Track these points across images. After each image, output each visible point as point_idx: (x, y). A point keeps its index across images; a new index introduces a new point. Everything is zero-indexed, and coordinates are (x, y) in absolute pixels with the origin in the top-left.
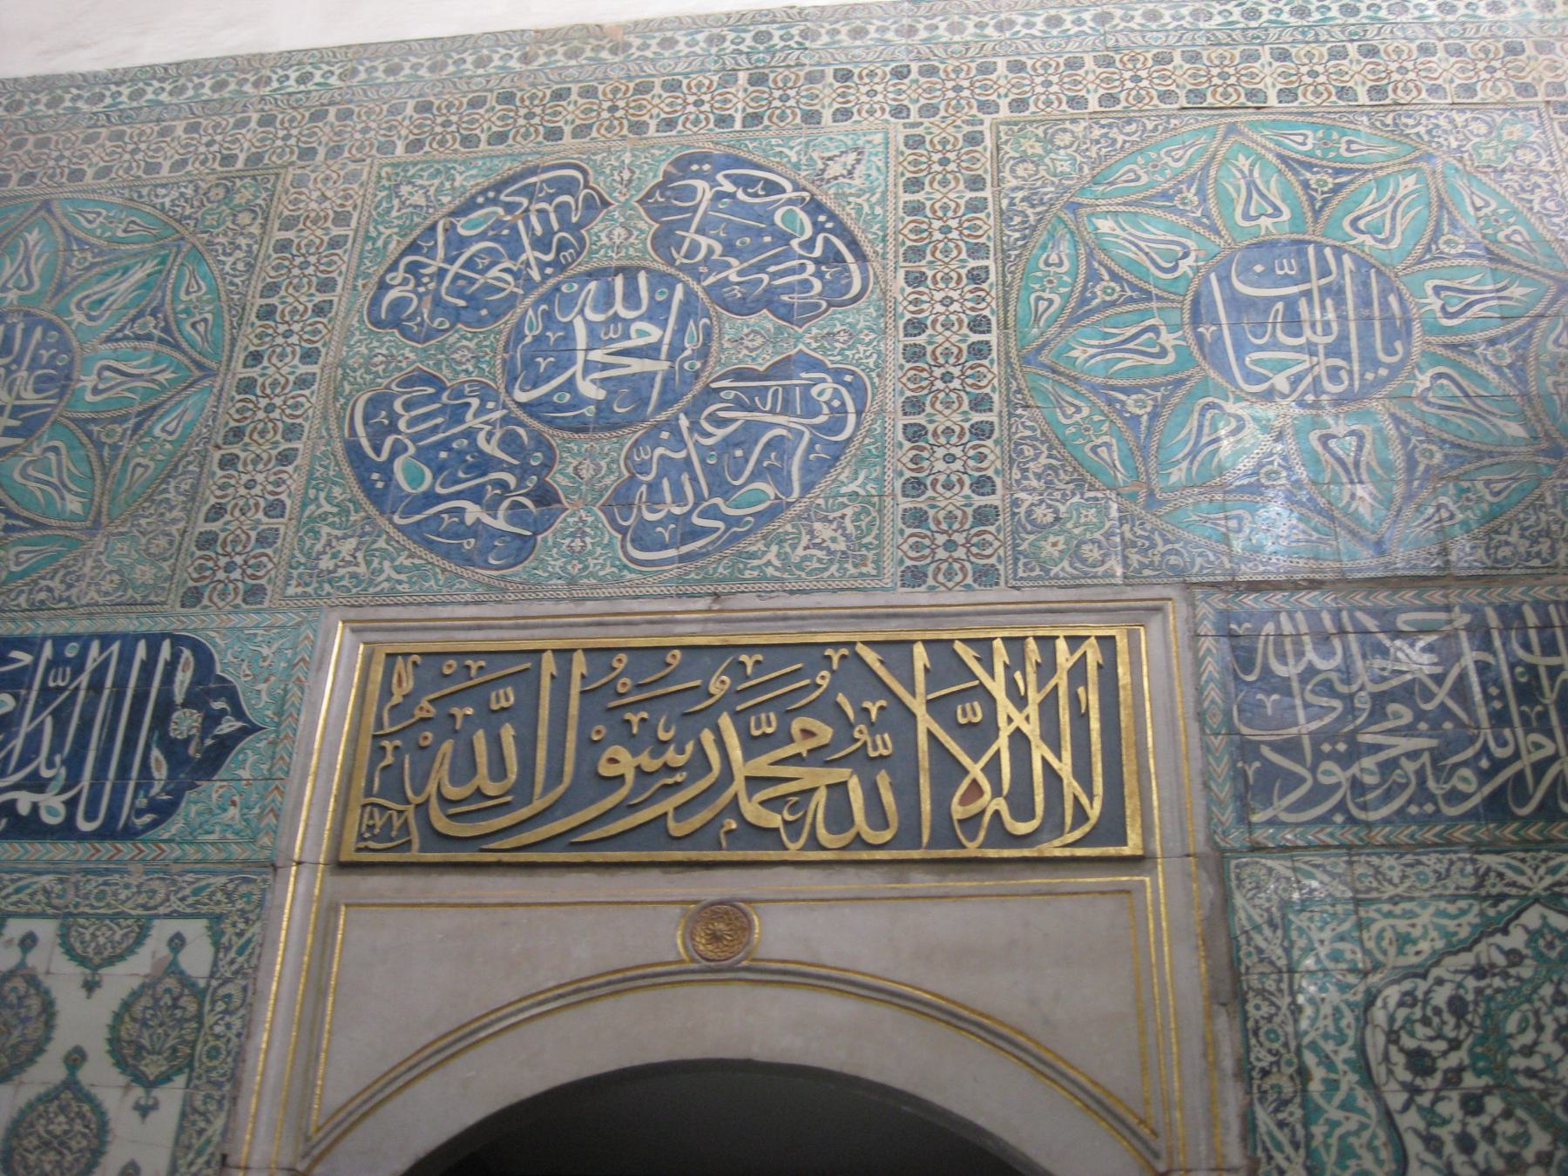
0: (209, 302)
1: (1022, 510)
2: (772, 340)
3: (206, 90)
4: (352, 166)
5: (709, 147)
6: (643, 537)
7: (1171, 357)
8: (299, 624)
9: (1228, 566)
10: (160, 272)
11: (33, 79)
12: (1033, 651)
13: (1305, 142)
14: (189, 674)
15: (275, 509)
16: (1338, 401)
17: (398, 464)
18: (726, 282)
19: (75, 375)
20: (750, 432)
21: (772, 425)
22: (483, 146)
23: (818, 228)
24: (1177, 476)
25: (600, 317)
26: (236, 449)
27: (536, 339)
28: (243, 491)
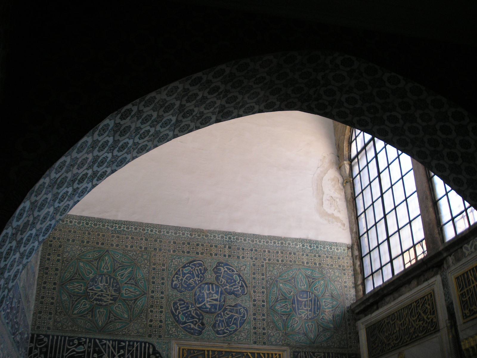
0: (143, 279)
1: (269, 333)
2: (234, 300)
3: (133, 229)
4: (164, 254)
5: (223, 261)
6: (218, 332)
7: (289, 310)
8: (168, 343)
9: (295, 344)
10: (133, 270)
11: (98, 218)
12: (270, 355)
13: (309, 273)
14: (152, 349)
15: (161, 321)
16: (310, 319)
17: (180, 315)
18: (226, 289)
19: (121, 290)
20: (232, 317)
21: (235, 316)
22: (186, 253)
23: (240, 280)
24: (289, 329)
25: (208, 292)
26: (152, 309)
27: (199, 295)
28: (155, 317)
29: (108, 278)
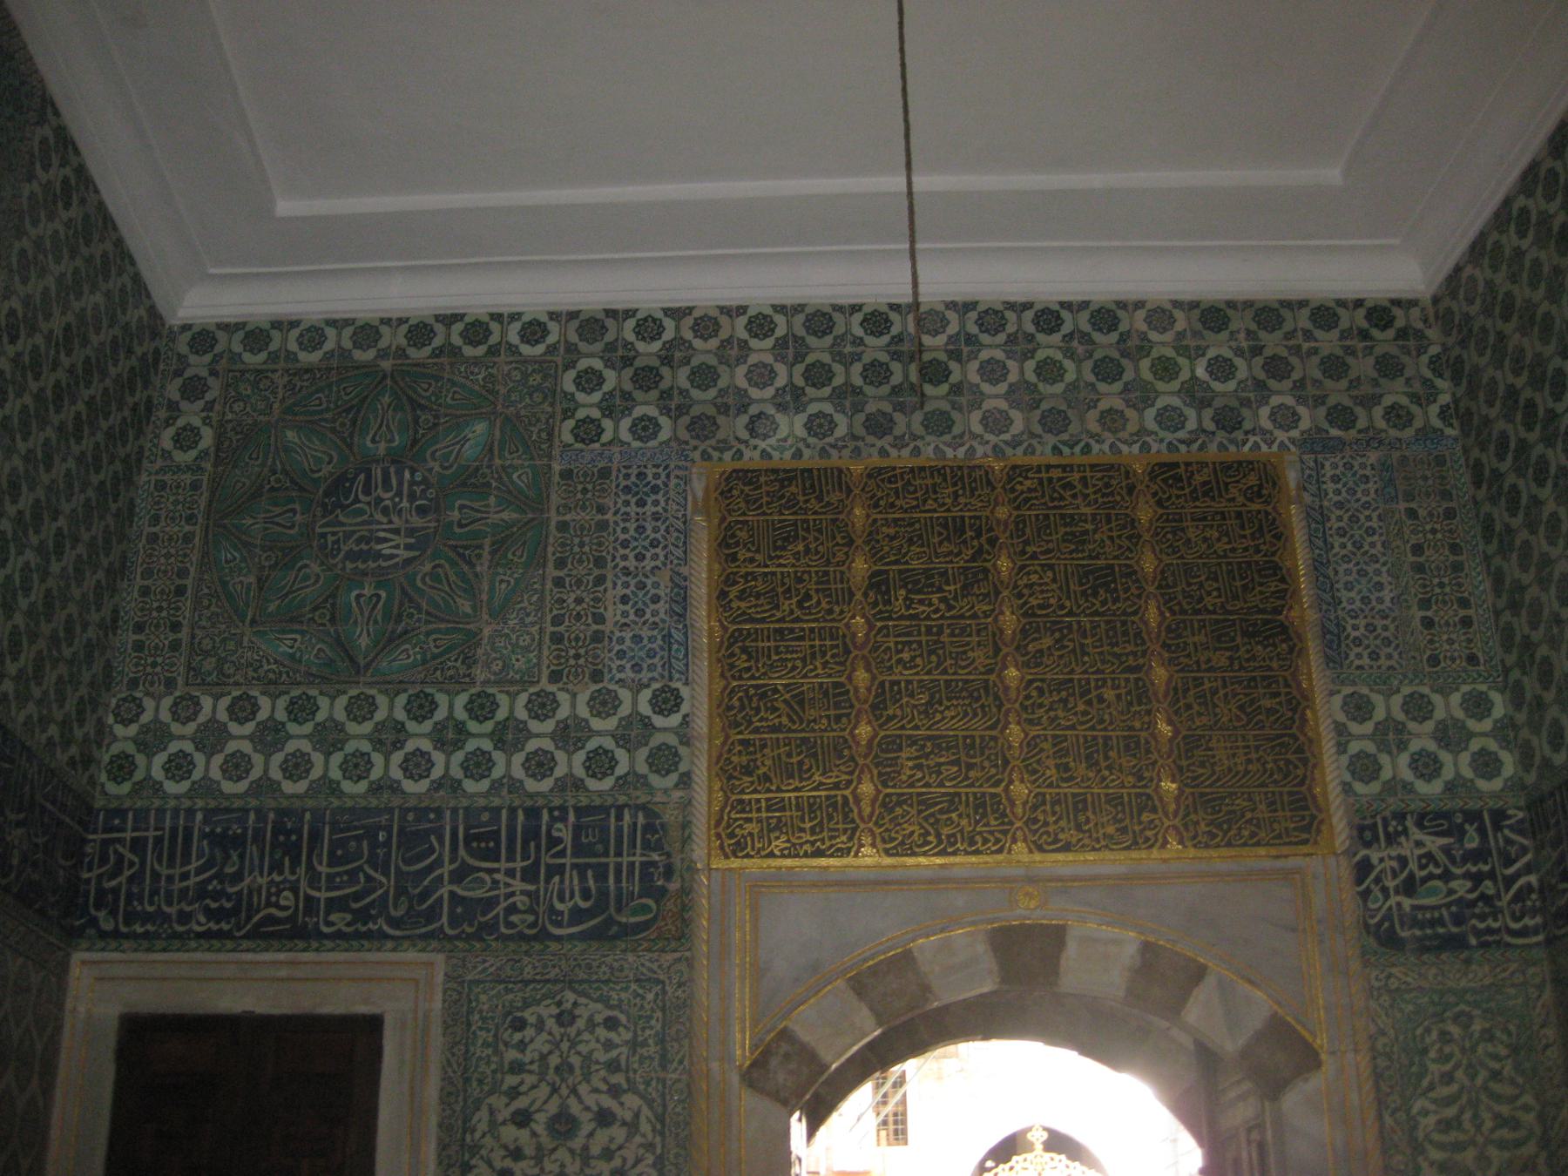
29: (392, 470)
